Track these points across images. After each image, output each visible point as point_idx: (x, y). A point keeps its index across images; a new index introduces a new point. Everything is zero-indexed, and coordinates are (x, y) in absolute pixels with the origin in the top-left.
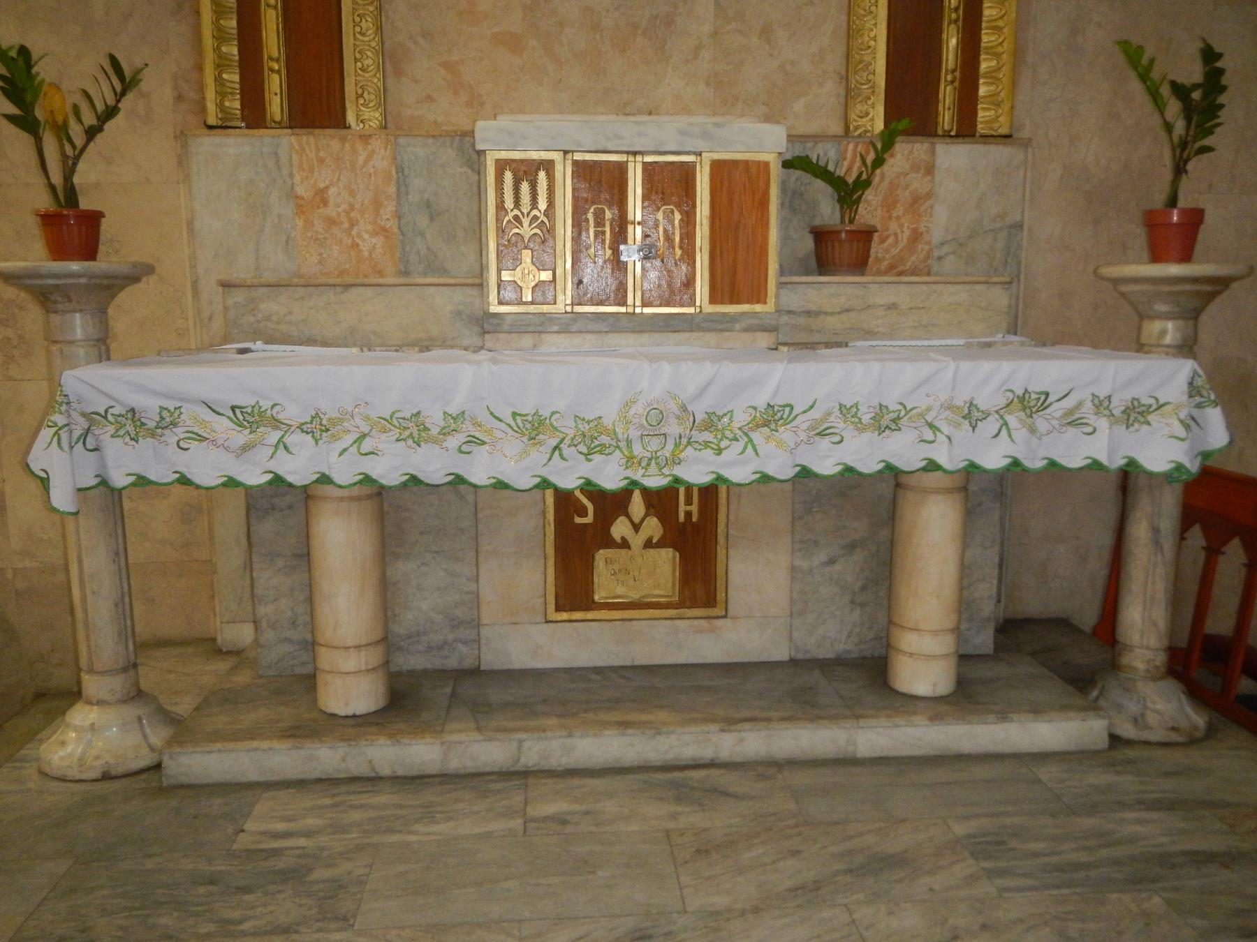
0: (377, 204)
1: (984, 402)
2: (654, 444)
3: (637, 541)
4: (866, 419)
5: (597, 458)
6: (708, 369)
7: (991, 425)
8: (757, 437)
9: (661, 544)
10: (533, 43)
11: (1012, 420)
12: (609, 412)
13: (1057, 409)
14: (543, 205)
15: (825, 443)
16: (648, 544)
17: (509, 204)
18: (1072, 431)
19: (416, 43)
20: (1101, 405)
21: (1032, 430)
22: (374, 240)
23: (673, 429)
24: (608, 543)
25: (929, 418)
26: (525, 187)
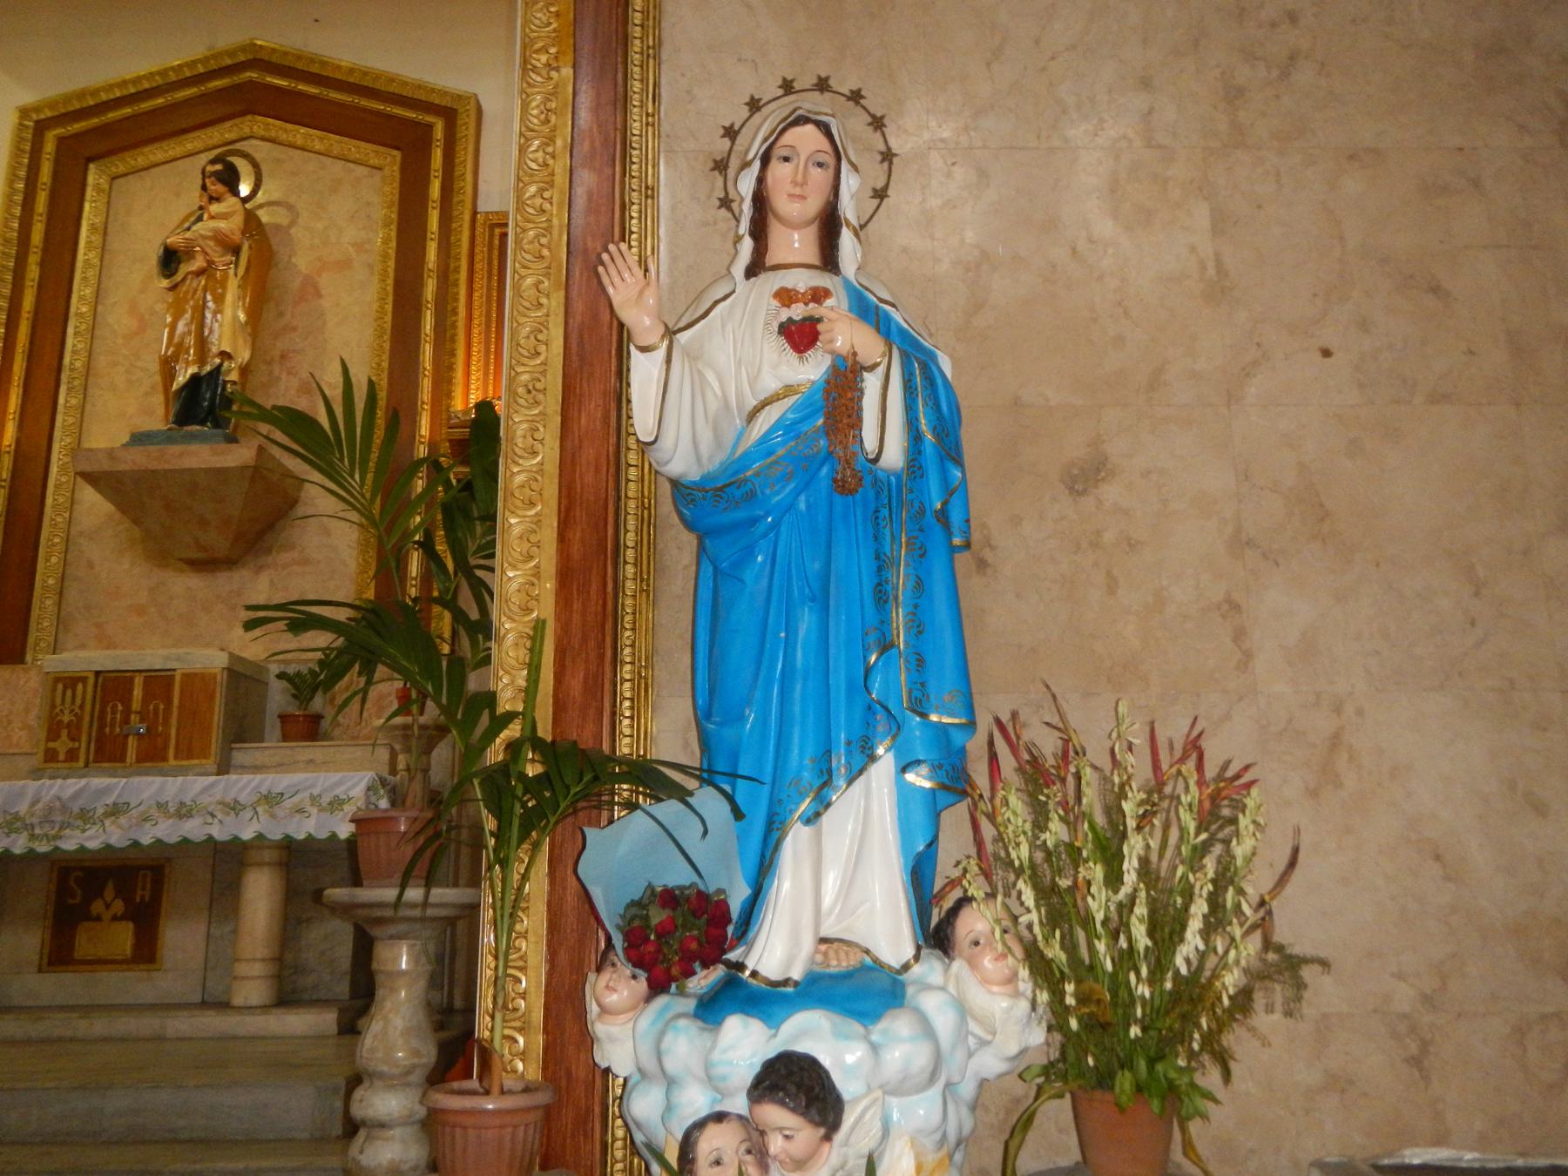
0: (27, 711)
1: (243, 798)
2: (47, 828)
3: (107, 916)
4: (172, 810)
5: (13, 836)
6: (83, 782)
7: (248, 814)
8: (107, 822)
9: (123, 918)
10: (153, 610)
11: (260, 810)
12: (23, 808)
13: (288, 804)
14: (78, 702)
15: (148, 825)
16: (115, 918)
17: (58, 701)
18: (298, 816)
19: (79, 613)
20: (314, 800)
21: (273, 816)
22: (22, 733)
23: (59, 818)
24: (88, 917)
25: (210, 809)
26: (69, 693)
